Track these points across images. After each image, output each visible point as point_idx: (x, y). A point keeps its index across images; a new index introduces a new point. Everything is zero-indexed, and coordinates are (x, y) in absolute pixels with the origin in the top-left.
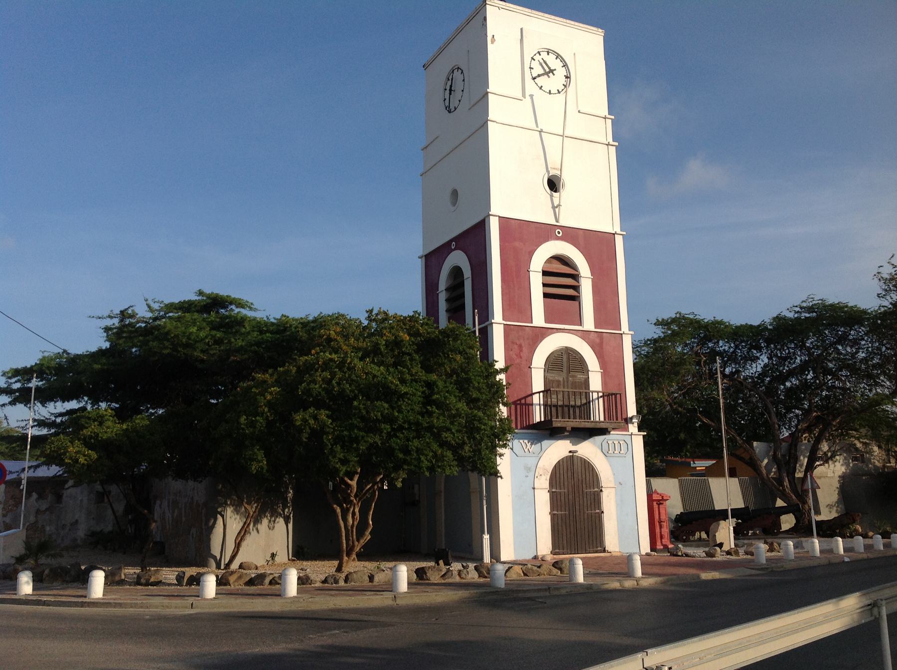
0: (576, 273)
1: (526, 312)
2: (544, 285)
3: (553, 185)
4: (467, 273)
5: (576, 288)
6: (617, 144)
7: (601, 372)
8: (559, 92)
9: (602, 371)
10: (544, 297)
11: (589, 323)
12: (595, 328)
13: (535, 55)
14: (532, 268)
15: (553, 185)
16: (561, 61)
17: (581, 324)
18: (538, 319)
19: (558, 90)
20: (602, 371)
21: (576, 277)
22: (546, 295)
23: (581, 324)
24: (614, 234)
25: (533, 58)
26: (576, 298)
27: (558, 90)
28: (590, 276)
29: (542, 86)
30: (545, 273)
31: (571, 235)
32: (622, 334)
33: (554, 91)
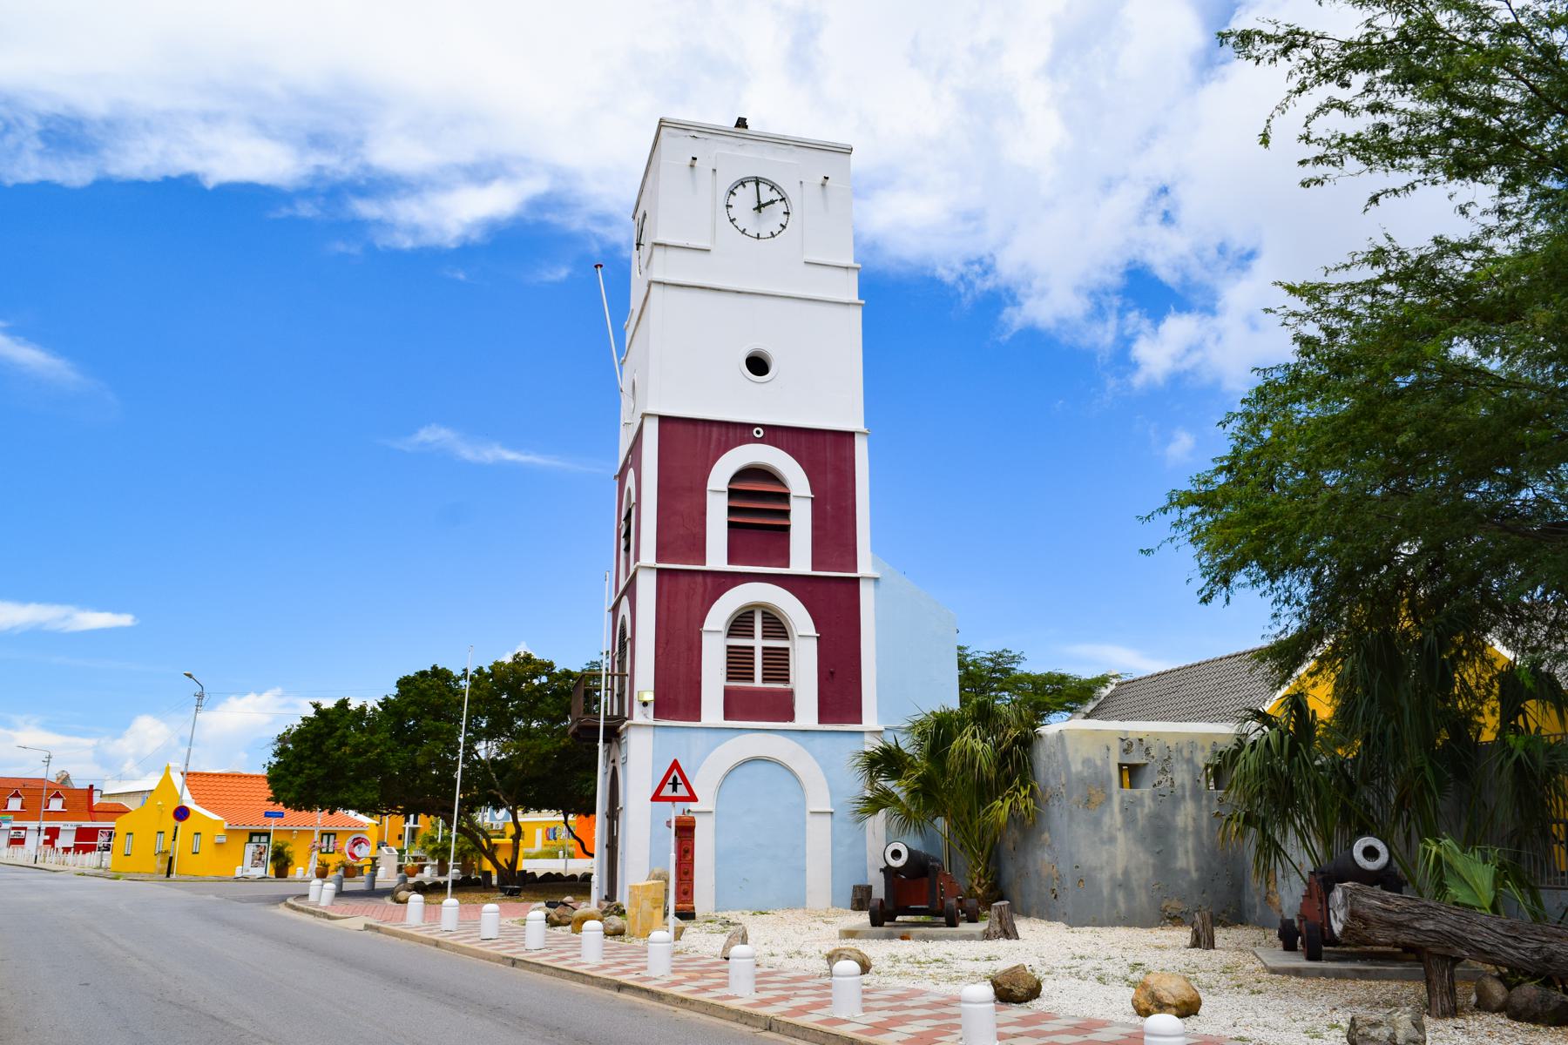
0: (781, 490)
1: (697, 548)
2: (732, 511)
3: (758, 365)
4: (633, 500)
5: (786, 514)
6: (863, 302)
7: (817, 637)
8: (773, 235)
9: (818, 635)
10: (729, 527)
11: (801, 561)
12: (813, 569)
13: (736, 187)
14: (708, 488)
15: (758, 365)
16: (779, 193)
17: (787, 565)
18: (717, 557)
19: (772, 233)
20: (818, 635)
21: (785, 497)
22: (731, 525)
23: (787, 565)
24: (852, 434)
25: (732, 192)
26: (786, 529)
27: (772, 233)
28: (809, 494)
29: (745, 230)
30: (732, 494)
31: (776, 435)
32: (857, 580)
33: (765, 233)
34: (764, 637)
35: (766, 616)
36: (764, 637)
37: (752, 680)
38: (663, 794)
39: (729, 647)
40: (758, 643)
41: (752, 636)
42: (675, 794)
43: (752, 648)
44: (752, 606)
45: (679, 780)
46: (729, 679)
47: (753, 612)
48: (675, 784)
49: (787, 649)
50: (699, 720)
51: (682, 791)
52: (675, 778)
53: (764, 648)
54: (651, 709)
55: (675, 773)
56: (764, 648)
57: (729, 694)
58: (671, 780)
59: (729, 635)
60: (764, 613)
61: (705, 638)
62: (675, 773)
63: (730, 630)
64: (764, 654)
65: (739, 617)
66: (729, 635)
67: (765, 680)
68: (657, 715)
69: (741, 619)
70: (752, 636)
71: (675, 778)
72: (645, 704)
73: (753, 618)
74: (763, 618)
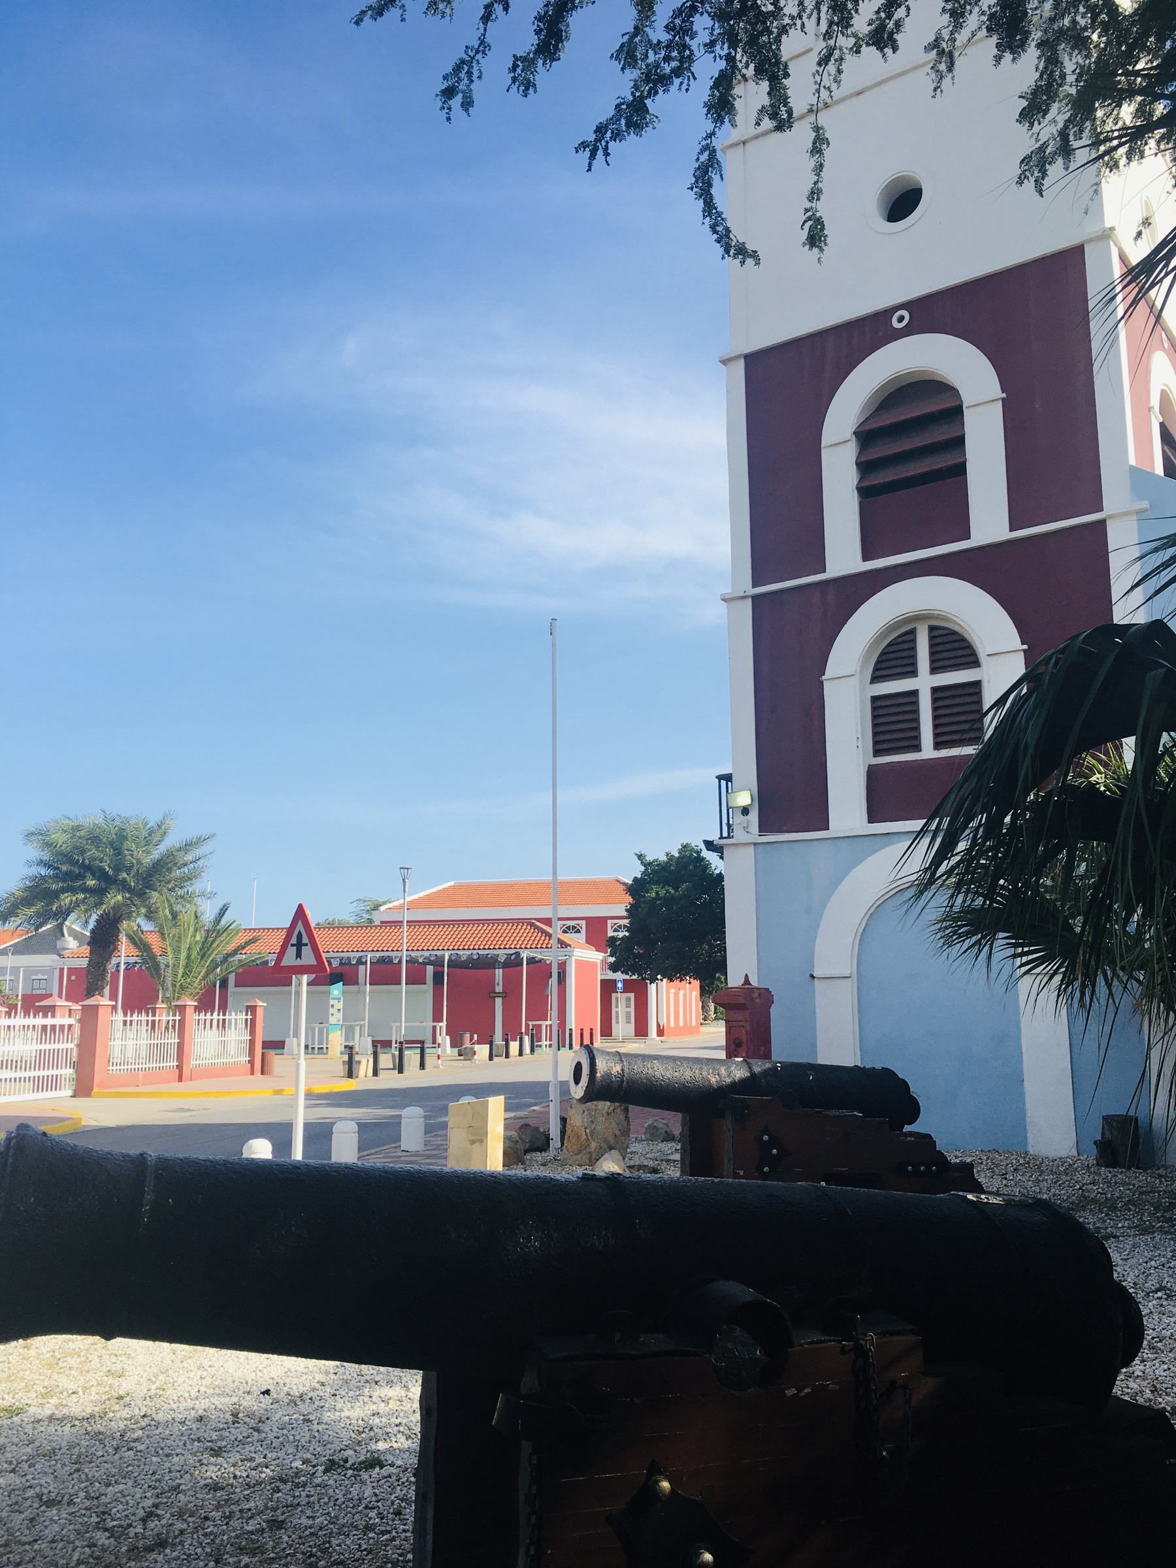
17: (967, 536)
21: (956, 412)
23: (967, 536)
26: (960, 470)
34: (934, 670)
35: (936, 633)
36: (934, 670)
37: (917, 748)
38: (286, 962)
39: (875, 699)
40: (924, 682)
41: (913, 673)
42: (299, 962)
43: (915, 693)
44: (919, 618)
45: (305, 940)
46: (877, 753)
47: (913, 632)
48: (299, 945)
49: (977, 684)
50: (826, 827)
51: (308, 958)
52: (300, 936)
53: (935, 690)
54: (754, 816)
55: (300, 927)
56: (935, 690)
57: (874, 776)
58: (294, 940)
59: (875, 679)
60: (932, 629)
61: (828, 688)
62: (300, 927)
63: (875, 670)
64: (934, 700)
65: (889, 645)
66: (875, 679)
67: (938, 746)
68: (764, 828)
69: (891, 649)
70: (913, 673)
71: (300, 936)
72: (745, 811)
73: (914, 641)
74: (931, 638)
